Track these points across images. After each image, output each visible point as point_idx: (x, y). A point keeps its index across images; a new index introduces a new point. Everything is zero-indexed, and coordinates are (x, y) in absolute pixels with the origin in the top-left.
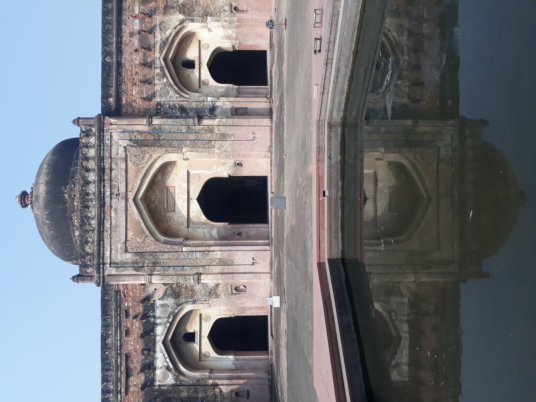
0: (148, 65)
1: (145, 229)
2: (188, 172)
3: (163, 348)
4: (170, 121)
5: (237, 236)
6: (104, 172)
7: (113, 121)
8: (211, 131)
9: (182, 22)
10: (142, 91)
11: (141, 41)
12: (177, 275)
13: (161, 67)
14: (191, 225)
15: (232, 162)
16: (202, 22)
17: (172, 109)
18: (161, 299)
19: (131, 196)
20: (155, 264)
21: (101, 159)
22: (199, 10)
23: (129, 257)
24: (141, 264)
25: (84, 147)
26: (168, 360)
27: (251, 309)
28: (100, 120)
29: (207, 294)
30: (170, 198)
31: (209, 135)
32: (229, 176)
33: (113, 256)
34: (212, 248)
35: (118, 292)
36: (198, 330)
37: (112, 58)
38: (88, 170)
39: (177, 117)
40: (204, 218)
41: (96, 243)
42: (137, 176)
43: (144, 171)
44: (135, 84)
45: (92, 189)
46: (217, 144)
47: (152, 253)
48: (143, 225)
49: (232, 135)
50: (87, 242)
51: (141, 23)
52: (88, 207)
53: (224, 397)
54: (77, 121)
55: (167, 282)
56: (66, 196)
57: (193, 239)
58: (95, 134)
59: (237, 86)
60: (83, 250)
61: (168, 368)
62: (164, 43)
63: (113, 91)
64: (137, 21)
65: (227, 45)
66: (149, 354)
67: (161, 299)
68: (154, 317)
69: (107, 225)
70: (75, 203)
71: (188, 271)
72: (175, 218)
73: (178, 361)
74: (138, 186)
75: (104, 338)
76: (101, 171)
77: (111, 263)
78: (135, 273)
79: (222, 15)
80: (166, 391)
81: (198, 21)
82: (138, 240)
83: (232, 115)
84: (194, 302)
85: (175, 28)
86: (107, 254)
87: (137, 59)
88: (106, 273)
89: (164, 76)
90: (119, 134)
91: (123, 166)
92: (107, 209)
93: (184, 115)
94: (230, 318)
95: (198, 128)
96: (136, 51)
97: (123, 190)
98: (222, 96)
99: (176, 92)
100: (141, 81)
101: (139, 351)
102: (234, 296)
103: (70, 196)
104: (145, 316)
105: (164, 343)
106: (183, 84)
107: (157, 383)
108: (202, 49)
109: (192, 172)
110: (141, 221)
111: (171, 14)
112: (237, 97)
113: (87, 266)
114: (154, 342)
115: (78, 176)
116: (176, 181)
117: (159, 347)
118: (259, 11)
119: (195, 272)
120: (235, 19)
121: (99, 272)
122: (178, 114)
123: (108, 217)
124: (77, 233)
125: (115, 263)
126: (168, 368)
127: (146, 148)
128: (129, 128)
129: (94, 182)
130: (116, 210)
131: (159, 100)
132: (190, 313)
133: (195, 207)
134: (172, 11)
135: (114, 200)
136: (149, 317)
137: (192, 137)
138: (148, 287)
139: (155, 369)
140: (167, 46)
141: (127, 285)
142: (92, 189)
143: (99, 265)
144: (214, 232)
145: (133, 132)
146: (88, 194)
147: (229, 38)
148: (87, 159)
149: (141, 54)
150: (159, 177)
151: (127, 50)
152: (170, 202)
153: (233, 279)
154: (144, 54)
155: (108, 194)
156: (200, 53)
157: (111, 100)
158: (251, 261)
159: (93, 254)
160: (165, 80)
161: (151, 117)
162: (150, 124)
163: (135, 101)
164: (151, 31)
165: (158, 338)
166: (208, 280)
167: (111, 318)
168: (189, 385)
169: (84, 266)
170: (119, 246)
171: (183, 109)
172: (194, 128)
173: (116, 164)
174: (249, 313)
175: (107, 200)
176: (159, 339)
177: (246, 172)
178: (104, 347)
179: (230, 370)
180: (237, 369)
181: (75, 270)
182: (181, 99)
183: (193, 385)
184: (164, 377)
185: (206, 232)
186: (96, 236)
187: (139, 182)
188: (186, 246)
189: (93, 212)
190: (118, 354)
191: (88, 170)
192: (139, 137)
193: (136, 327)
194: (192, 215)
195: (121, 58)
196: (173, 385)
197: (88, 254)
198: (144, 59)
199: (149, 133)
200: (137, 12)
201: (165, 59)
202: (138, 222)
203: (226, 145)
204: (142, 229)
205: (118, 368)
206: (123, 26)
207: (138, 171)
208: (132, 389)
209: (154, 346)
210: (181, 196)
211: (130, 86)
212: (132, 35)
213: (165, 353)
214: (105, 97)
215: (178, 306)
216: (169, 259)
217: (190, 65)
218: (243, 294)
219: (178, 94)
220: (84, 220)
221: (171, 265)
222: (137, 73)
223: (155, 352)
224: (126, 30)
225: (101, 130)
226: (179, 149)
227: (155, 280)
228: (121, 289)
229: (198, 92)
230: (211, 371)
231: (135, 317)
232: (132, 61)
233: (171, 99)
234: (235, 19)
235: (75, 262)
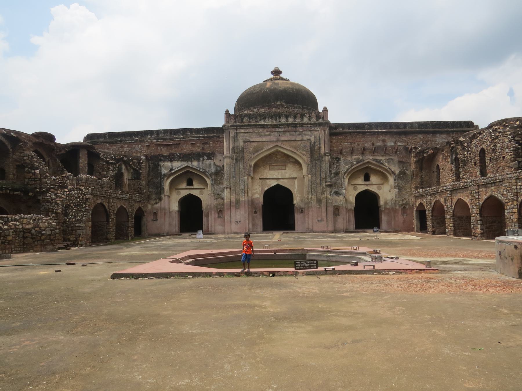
0: (364, 151)
1: (259, 153)
2: (296, 178)
3: (184, 166)
4: (328, 167)
5: (254, 210)
6: (294, 127)
7: (327, 131)
8: (322, 193)
9: (393, 173)
10: (347, 149)
11: (379, 147)
12: (230, 173)
13: (363, 160)
14: (261, 181)
15: (302, 206)
16: (395, 186)
17: (336, 167)
18: (215, 164)
19: (279, 144)
20: (237, 160)
21: (302, 125)
22: (402, 183)
23: (242, 144)
24: (236, 151)
25: (309, 115)
26: (177, 169)
27: (208, 221)
28: (328, 124)
29: (217, 193)
30: (279, 167)
31: (320, 191)
32: (294, 205)
33: (241, 134)
34: (246, 195)
35: (219, 137)
36: (195, 187)
37: (368, 129)
38: (295, 117)
39: (330, 171)
40: (266, 189)
41: (249, 124)
42: (292, 147)
43: (295, 151)
44: (351, 144)
45: (283, 121)
46: (314, 198)
47: (243, 158)
48: (261, 151)
49: (320, 207)
50: (250, 118)
51: (391, 147)
52: (272, 118)
53: (153, 205)
54: (325, 110)
55: (225, 167)
56: (279, 103)
57: (252, 182)
58: (317, 121)
59: (353, 208)
60: (244, 117)
61: (171, 170)
62: (379, 161)
63: (347, 130)
64: (393, 144)
65: (382, 202)
66: (180, 158)
67: (215, 164)
68: (203, 160)
69: (260, 130)
70: (274, 109)
71: (233, 180)
72: (265, 171)
73: (175, 175)
74: (285, 147)
75: (191, 130)
76: (295, 126)
77: (237, 133)
78: (231, 148)
79: (400, 199)
80: (158, 170)
81: (395, 183)
82: (251, 149)
83: (334, 206)
84: (212, 184)
85: (389, 169)
86: (243, 131)
87: (368, 145)
88: (231, 131)
89: (358, 162)
90: (318, 135)
91: (298, 139)
92: (270, 129)
93: (333, 175)
94: (202, 207)
95: (324, 184)
96: (373, 144)
97: (283, 138)
98: (346, 200)
99: (347, 170)
100: (353, 148)
101: (182, 152)
102: (216, 209)
103: (278, 105)
104: (204, 154)
105: (187, 167)
106: (353, 174)
107: (162, 163)
108: (377, 186)
109: (296, 181)
110: (264, 150)
111: (399, 166)
112: (346, 209)
113: (235, 119)
114: (187, 161)
115: (291, 110)
116: (290, 172)
117: (185, 164)
118: (403, 223)
119: (232, 184)
120: (398, 207)
121: (231, 126)
122: (333, 172)
123: (265, 131)
124: (255, 110)
125: (237, 135)
126: (171, 170)
127: (310, 152)
128: (322, 142)
129: (287, 121)
130: (269, 135)
131: (342, 159)
132: (205, 183)
133: (273, 183)
134: (401, 166)
135: (276, 134)
136: (203, 157)
137: (318, 181)
138: (222, 156)
139: (171, 161)
140: (378, 164)
141: (223, 142)
142: (283, 121)
143: (236, 126)
144: (256, 196)
145: (320, 144)
146: (280, 118)
147: (386, 203)
148: (302, 116)
149: (371, 147)
150: (292, 160)
151: (374, 139)
152: (276, 167)
153: (227, 209)
154: (371, 149)
155: (280, 130)
156: (374, 185)
157: (341, 129)
158: (238, 221)
159: (242, 122)
160: (355, 163)
161: (330, 155)
162: (325, 154)
163: (341, 144)
164: (385, 154)
165: (190, 163)
166: (226, 194)
167: (202, 134)
168: (161, 183)
169: (235, 116)
170: (247, 138)
171: (337, 174)
172: (324, 182)
173: (300, 134)
174: (205, 219)
175: (277, 130)
176: (189, 164)
177: (298, 217)
178: (185, 131)
179: (169, 209)
180: (170, 212)
181: (232, 112)
182: (343, 173)
183: (161, 185)
184: (165, 167)
185: (257, 191)
186: (253, 123)
187: (288, 148)
188: (248, 178)
189: (268, 122)
190: (180, 138)
191: (295, 117)
192: (316, 148)
193: (198, 149)
194: (268, 181)
195: (368, 135)
196: (161, 173)
197: (242, 119)
198: (367, 149)
199: (320, 153)
200: (399, 144)
201: (368, 162)
202: (262, 149)
203: (314, 203)
204: (258, 151)
205: (172, 139)
206: (389, 136)
207: (295, 148)
208: (159, 148)
209: (185, 161)
210: (280, 174)
211: (350, 141)
212: (384, 141)
213: (181, 167)
214: (342, 125)
215: (210, 175)
216: (240, 168)
217: (367, 178)
218: (217, 215)
219: (346, 172)
220: (263, 116)
221: (236, 169)
222: (359, 145)
223: (182, 161)
224: (387, 138)
225: (320, 125)
226: (310, 172)
227: (227, 161)
228: (221, 139)
229: (348, 184)
230: (169, 197)
231: (203, 149)
232: (366, 142)
233: (342, 167)
234: (398, 207)
235: (237, 107)
